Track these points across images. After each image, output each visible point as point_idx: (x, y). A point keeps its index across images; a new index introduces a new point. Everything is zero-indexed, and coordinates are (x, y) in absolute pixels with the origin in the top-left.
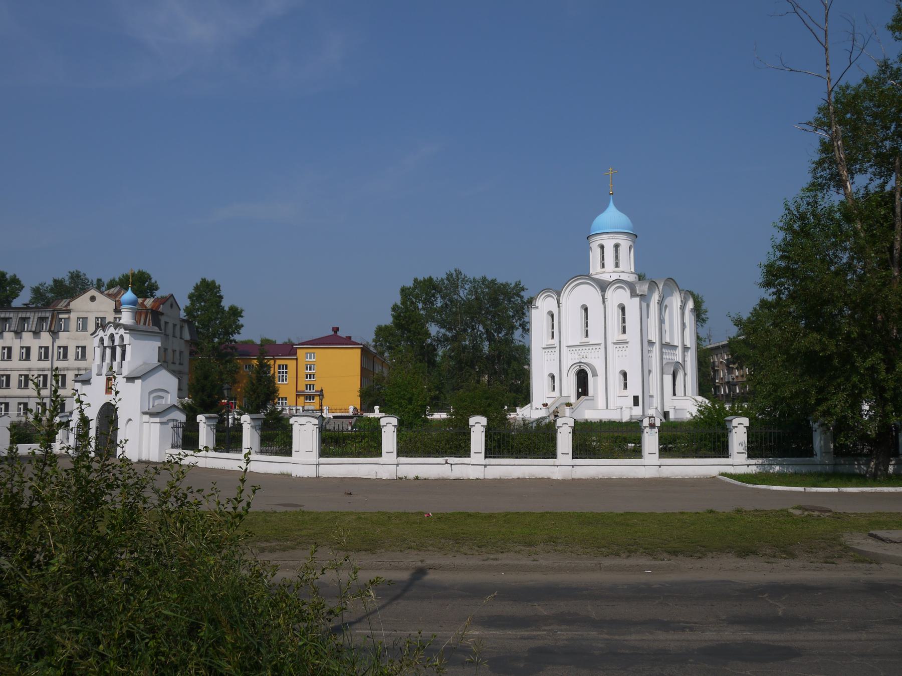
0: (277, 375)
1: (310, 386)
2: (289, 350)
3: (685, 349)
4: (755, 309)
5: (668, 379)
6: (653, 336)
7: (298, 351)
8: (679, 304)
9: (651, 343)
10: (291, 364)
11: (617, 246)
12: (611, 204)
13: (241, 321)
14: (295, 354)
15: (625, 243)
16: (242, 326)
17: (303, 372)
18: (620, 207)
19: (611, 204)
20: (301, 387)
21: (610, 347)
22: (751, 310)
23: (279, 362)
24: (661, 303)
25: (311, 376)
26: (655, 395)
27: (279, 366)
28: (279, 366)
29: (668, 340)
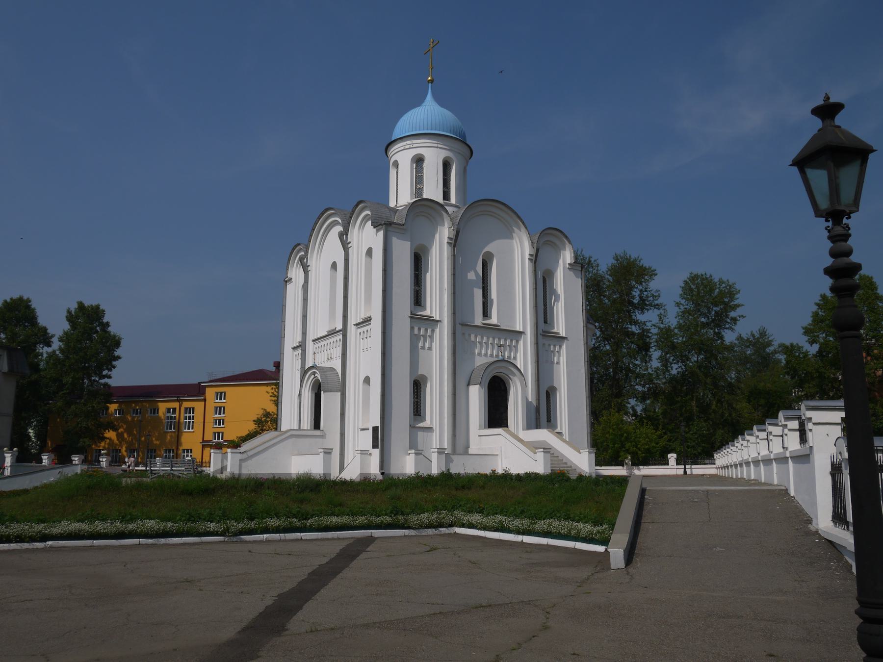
0: (182, 420)
1: (217, 435)
2: (197, 391)
3: (545, 336)
4: (824, 297)
5: (476, 396)
6: (438, 304)
7: (207, 390)
8: (528, 250)
9: (432, 322)
10: (198, 406)
11: (419, 161)
12: (429, 96)
13: (118, 352)
14: (204, 394)
15: (435, 156)
16: (119, 358)
17: (211, 415)
18: (440, 100)
19: (429, 96)
20: (209, 436)
21: (352, 330)
22: (817, 299)
23: (186, 405)
24: (455, 242)
25: (219, 421)
26: (436, 426)
27: (186, 409)
28: (186, 409)
29: (494, 320)
